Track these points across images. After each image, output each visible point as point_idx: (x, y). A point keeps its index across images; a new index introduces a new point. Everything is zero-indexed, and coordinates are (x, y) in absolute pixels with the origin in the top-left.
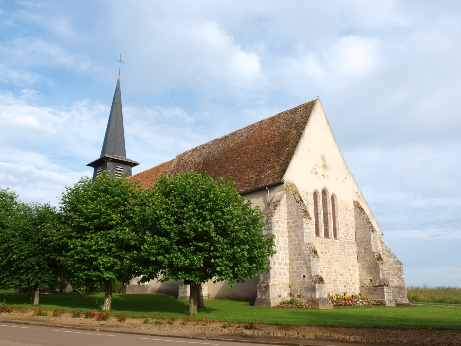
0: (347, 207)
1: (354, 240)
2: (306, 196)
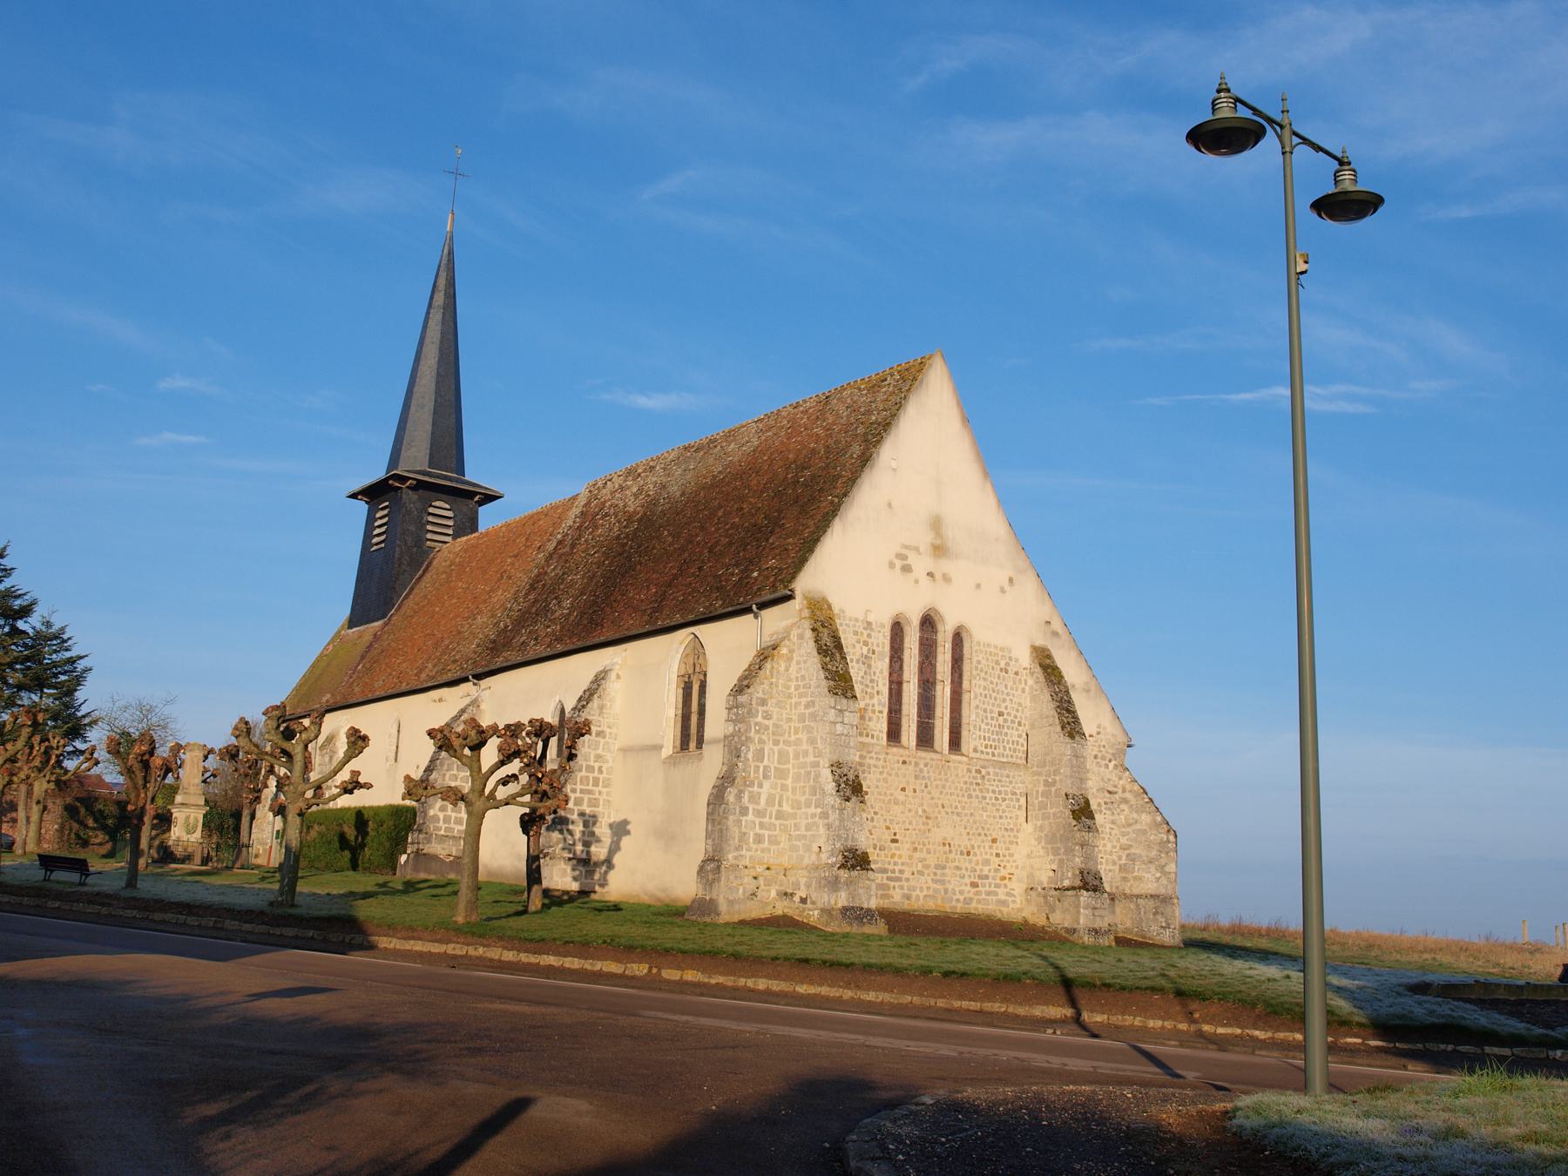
2: (865, 633)
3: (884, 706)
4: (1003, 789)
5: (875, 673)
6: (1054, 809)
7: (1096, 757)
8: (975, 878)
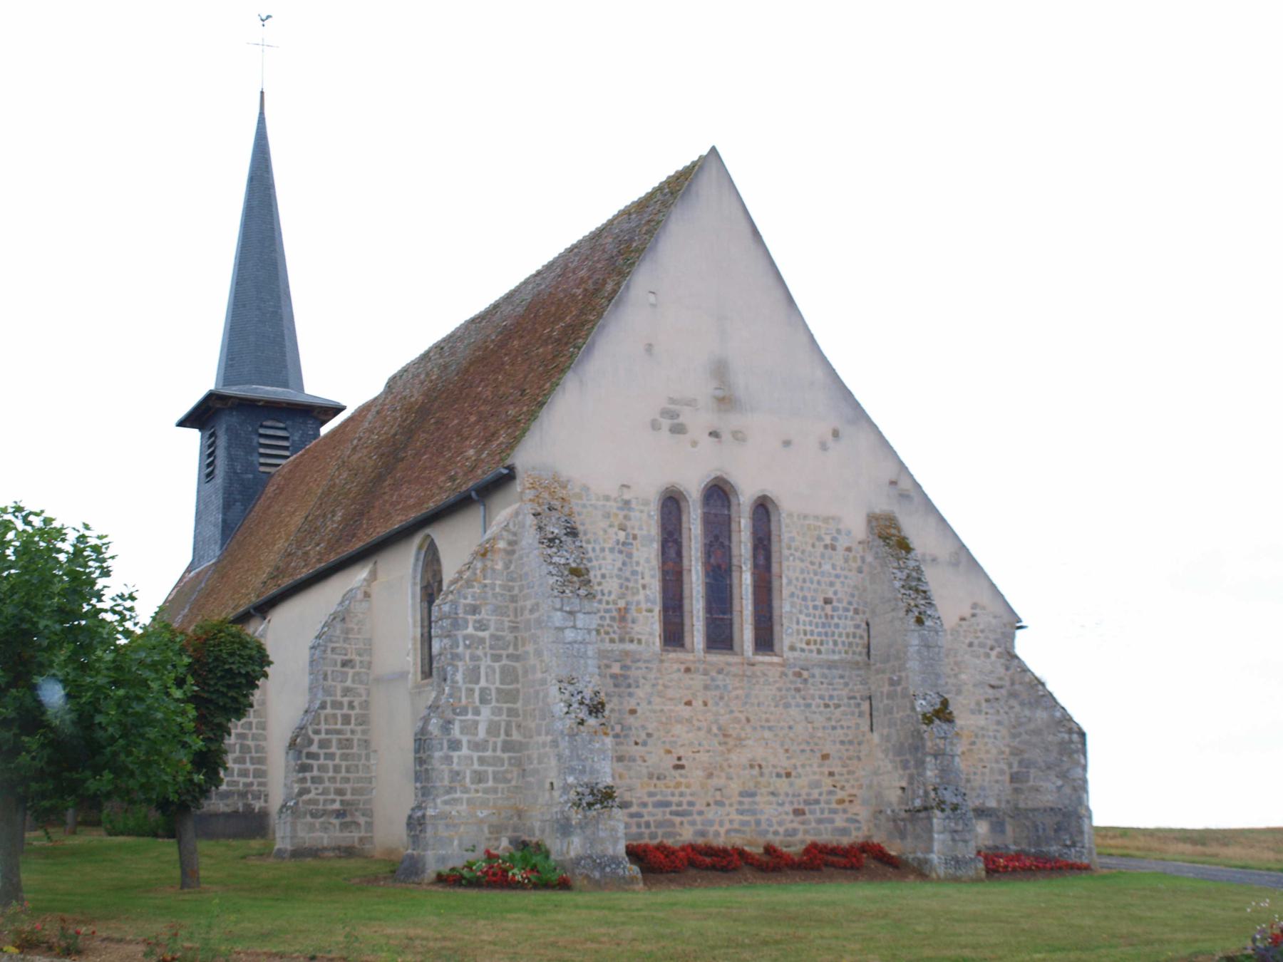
0: (834, 539)
1: (860, 654)
2: (621, 514)
3: (654, 602)
4: (835, 693)
5: (638, 564)
6: (901, 714)
7: (971, 645)
8: (799, 804)
